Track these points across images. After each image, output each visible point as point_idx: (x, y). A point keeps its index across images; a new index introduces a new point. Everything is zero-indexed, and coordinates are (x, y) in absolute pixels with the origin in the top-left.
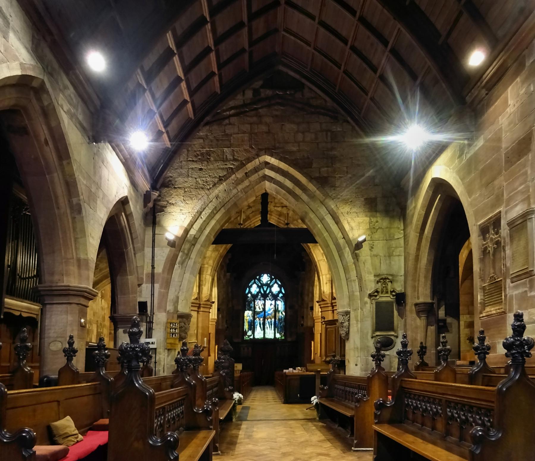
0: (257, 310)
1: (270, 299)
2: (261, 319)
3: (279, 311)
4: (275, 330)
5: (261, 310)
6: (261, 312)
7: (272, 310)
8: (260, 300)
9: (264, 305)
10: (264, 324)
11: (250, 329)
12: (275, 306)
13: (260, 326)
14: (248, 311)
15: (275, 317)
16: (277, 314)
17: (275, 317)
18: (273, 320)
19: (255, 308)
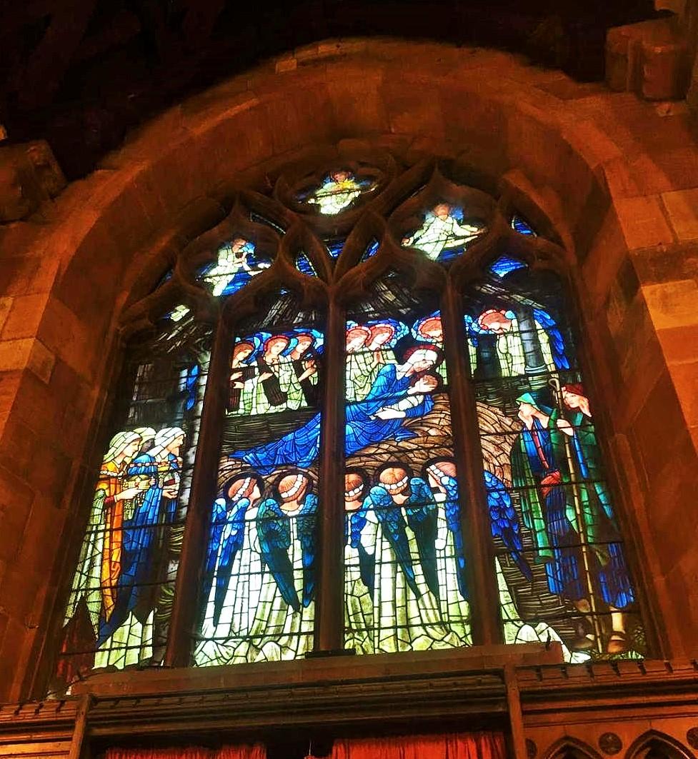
0: (253, 399)
1: (389, 314)
2: (293, 484)
3: (508, 393)
4: (476, 586)
5: (296, 401)
6: (294, 420)
7: (423, 386)
8: (283, 329)
9: (331, 361)
10: (327, 531)
11: (132, 595)
12: (452, 350)
13: (277, 564)
14: (148, 433)
15: (463, 446)
16: (489, 417)
17: (463, 446)
18: (442, 475)
19: (225, 395)
